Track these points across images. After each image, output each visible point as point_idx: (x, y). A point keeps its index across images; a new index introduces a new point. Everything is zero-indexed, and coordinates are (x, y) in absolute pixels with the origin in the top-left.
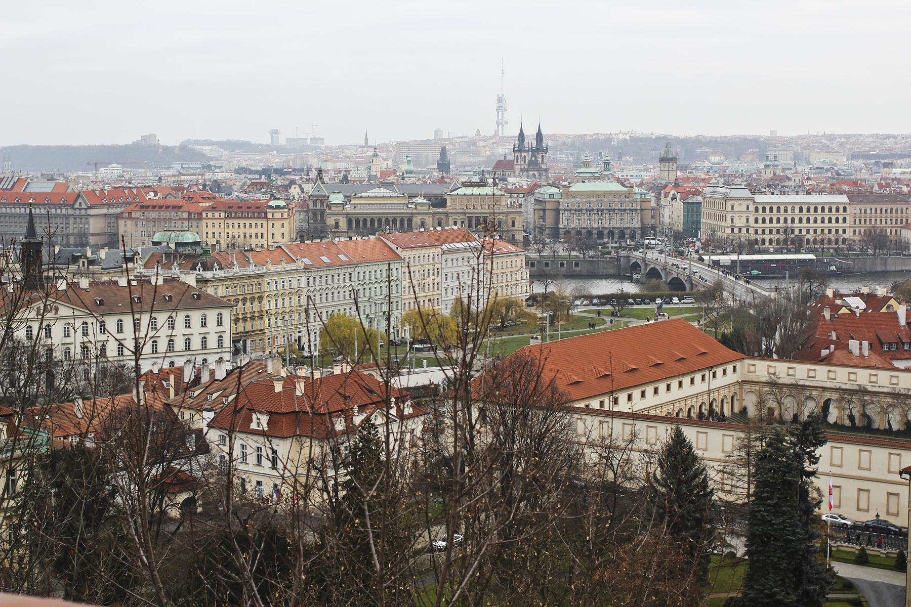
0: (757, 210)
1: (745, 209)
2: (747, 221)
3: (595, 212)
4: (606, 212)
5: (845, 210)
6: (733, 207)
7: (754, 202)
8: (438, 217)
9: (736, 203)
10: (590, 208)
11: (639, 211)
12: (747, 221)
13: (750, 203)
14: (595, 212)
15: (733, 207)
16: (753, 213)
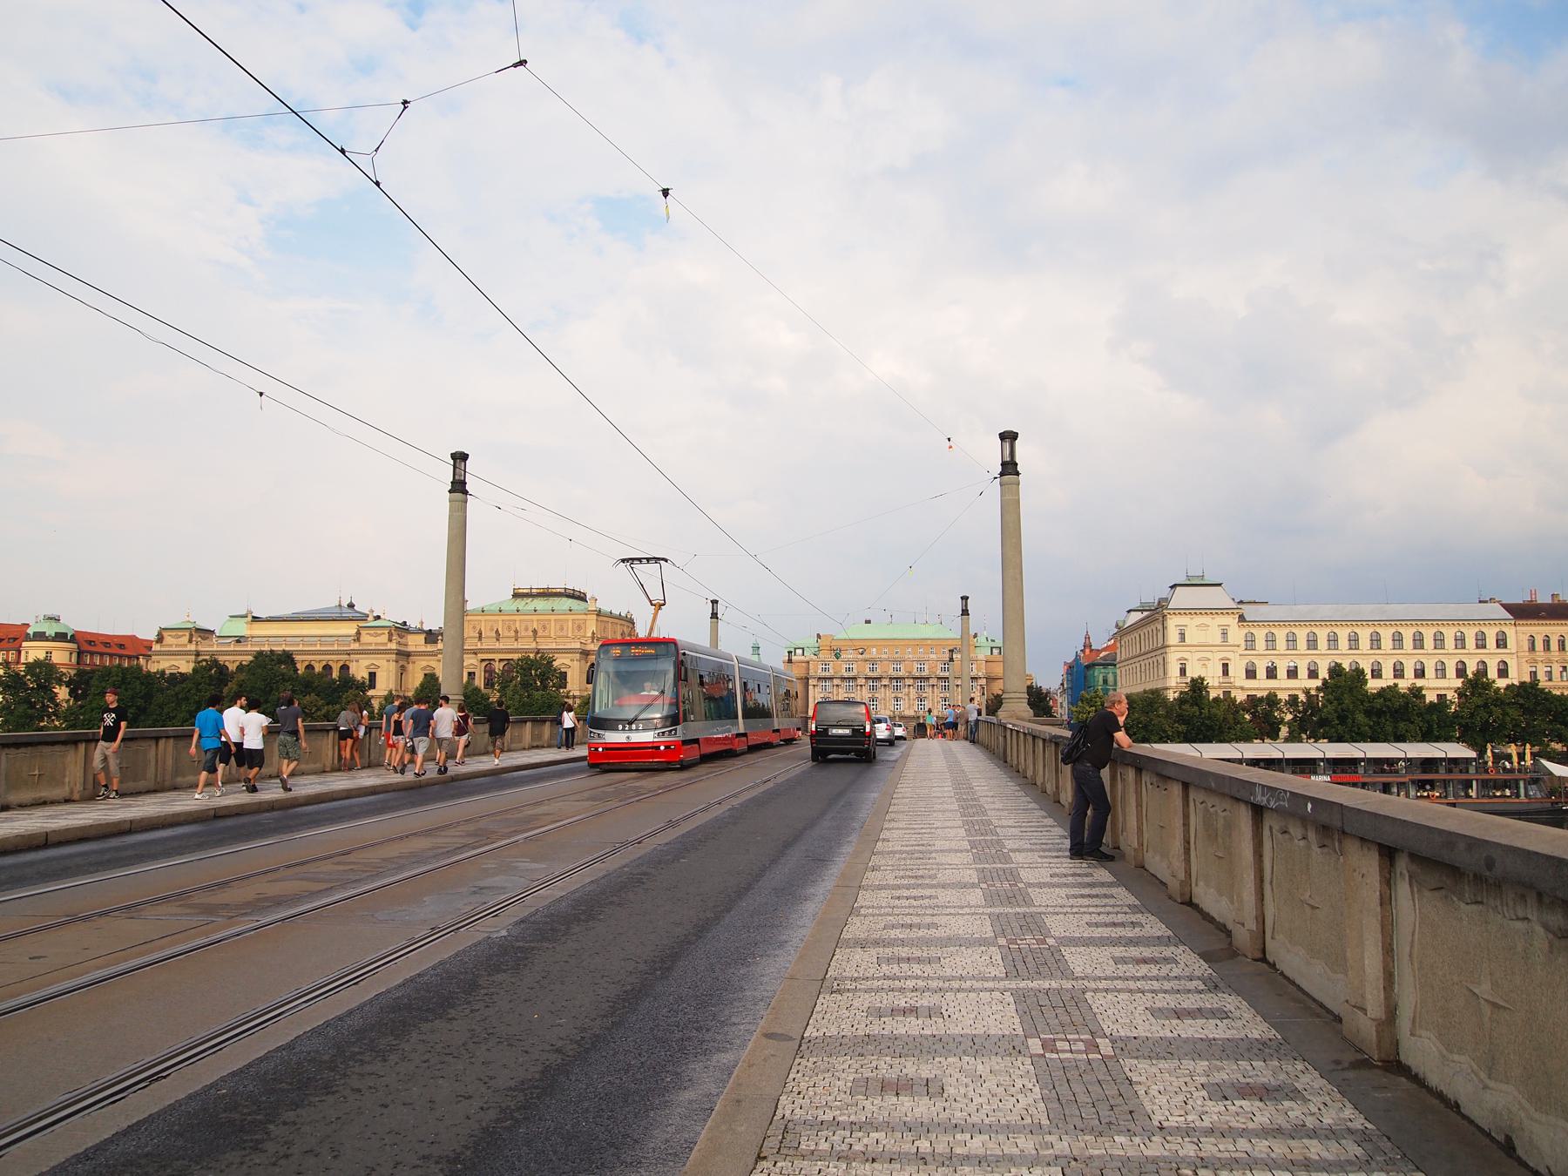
0: (1250, 642)
1: (1218, 640)
2: (1226, 672)
3: (885, 682)
4: (911, 682)
5: (1501, 642)
6: (1182, 636)
7: (1242, 618)
8: (424, 664)
9: (1191, 623)
10: (875, 674)
11: (983, 682)
12: (1226, 672)
13: (1232, 621)
14: (885, 682)
15: (1182, 636)
16: (1241, 650)
